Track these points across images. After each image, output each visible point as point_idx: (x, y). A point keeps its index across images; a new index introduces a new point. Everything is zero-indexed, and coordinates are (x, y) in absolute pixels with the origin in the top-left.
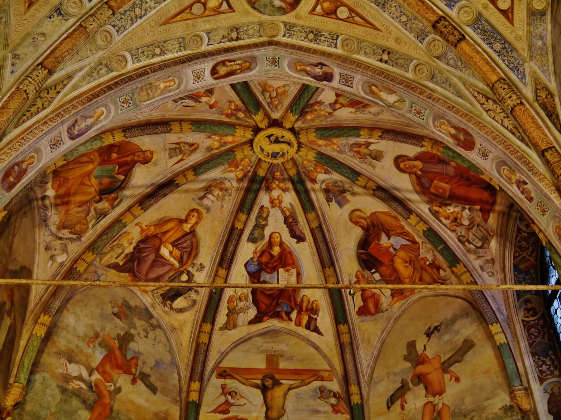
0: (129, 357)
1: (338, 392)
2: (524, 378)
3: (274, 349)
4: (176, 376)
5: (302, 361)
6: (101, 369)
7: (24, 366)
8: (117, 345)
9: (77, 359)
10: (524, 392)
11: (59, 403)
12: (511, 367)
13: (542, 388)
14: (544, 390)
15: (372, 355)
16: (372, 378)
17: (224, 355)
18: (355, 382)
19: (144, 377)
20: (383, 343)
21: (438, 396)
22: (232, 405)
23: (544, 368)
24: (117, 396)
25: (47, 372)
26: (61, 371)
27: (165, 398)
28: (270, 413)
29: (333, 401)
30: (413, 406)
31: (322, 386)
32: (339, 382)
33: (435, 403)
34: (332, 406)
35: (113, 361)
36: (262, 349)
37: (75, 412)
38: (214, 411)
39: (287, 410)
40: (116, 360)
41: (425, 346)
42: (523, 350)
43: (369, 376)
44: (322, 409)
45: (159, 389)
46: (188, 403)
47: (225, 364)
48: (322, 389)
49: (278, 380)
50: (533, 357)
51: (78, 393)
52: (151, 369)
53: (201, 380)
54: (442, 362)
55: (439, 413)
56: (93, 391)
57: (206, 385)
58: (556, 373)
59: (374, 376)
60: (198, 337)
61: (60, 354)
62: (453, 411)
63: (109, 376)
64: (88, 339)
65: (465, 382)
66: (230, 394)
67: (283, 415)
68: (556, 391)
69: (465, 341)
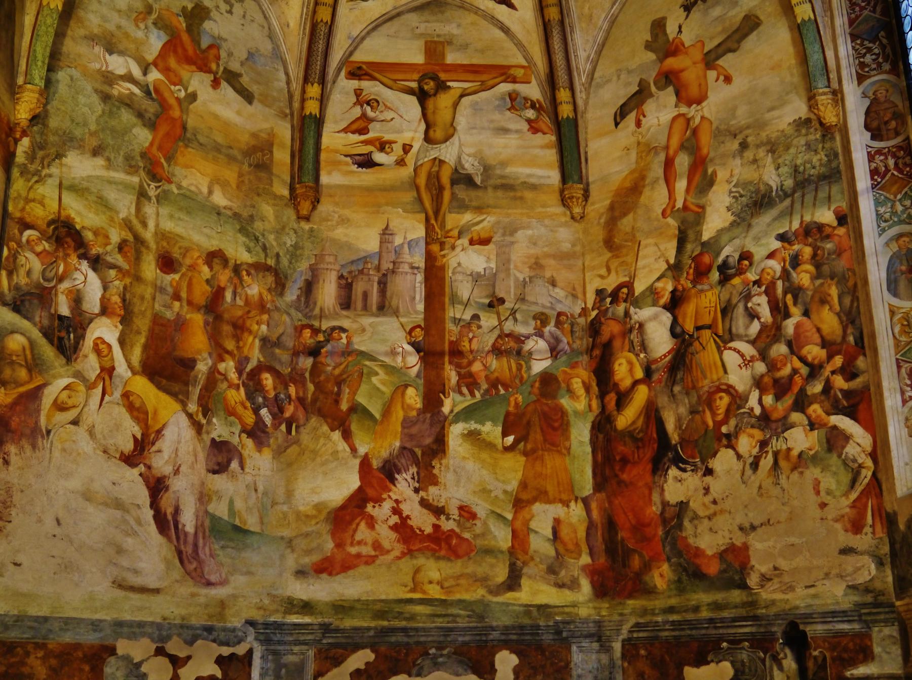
0: (204, 45)
1: (538, 100)
2: (833, 76)
3: (438, 32)
4: (283, 76)
5: (482, 52)
6: (161, 64)
7: (36, 57)
8: (184, 25)
9: (121, 47)
10: (830, 96)
11: (100, 116)
12: (815, 57)
13: (859, 91)
14: (863, 93)
15: (595, 42)
16: (592, 79)
17: (357, 43)
18: (567, 84)
19: (232, 78)
20: (613, 22)
21: (694, 106)
22: (371, 120)
23: (868, 59)
24: (191, 107)
25: (76, 68)
26: (98, 66)
27: (267, 109)
28: (431, 132)
29: (531, 114)
30: (656, 121)
31: (514, 91)
32: (540, 84)
33: (690, 116)
34: (529, 121)
35: (180, 50)
36: (418, 31)
37: (127, 131)
38: (345, 130)
39: (458, 128)
40: (185, 50)
41: (680, 27)
42: (839, 30)
43: (588, 75)
44: (512, 126)
45: (256, 95)
46: (303, 118)
47: (359, 57)
48: (514, 96)
49: (444, 82)
50: (852, 42)
51: (128, 102)
52: (242, 64)
53: (322, 82)
54: (705, 51)
55: (695, 132)
56: (152, 99)
57: (331, 91)
58: (887, 67)
59: (596, 75)
60: (314, 12)
61: (92, 39)
62: (717, 128)
63: (176, 76)
64: (136, 14)
65: (740, 84)
66: (368, 103)
67: (453, 135)
68: (881, 95)
69: (747, 18)
